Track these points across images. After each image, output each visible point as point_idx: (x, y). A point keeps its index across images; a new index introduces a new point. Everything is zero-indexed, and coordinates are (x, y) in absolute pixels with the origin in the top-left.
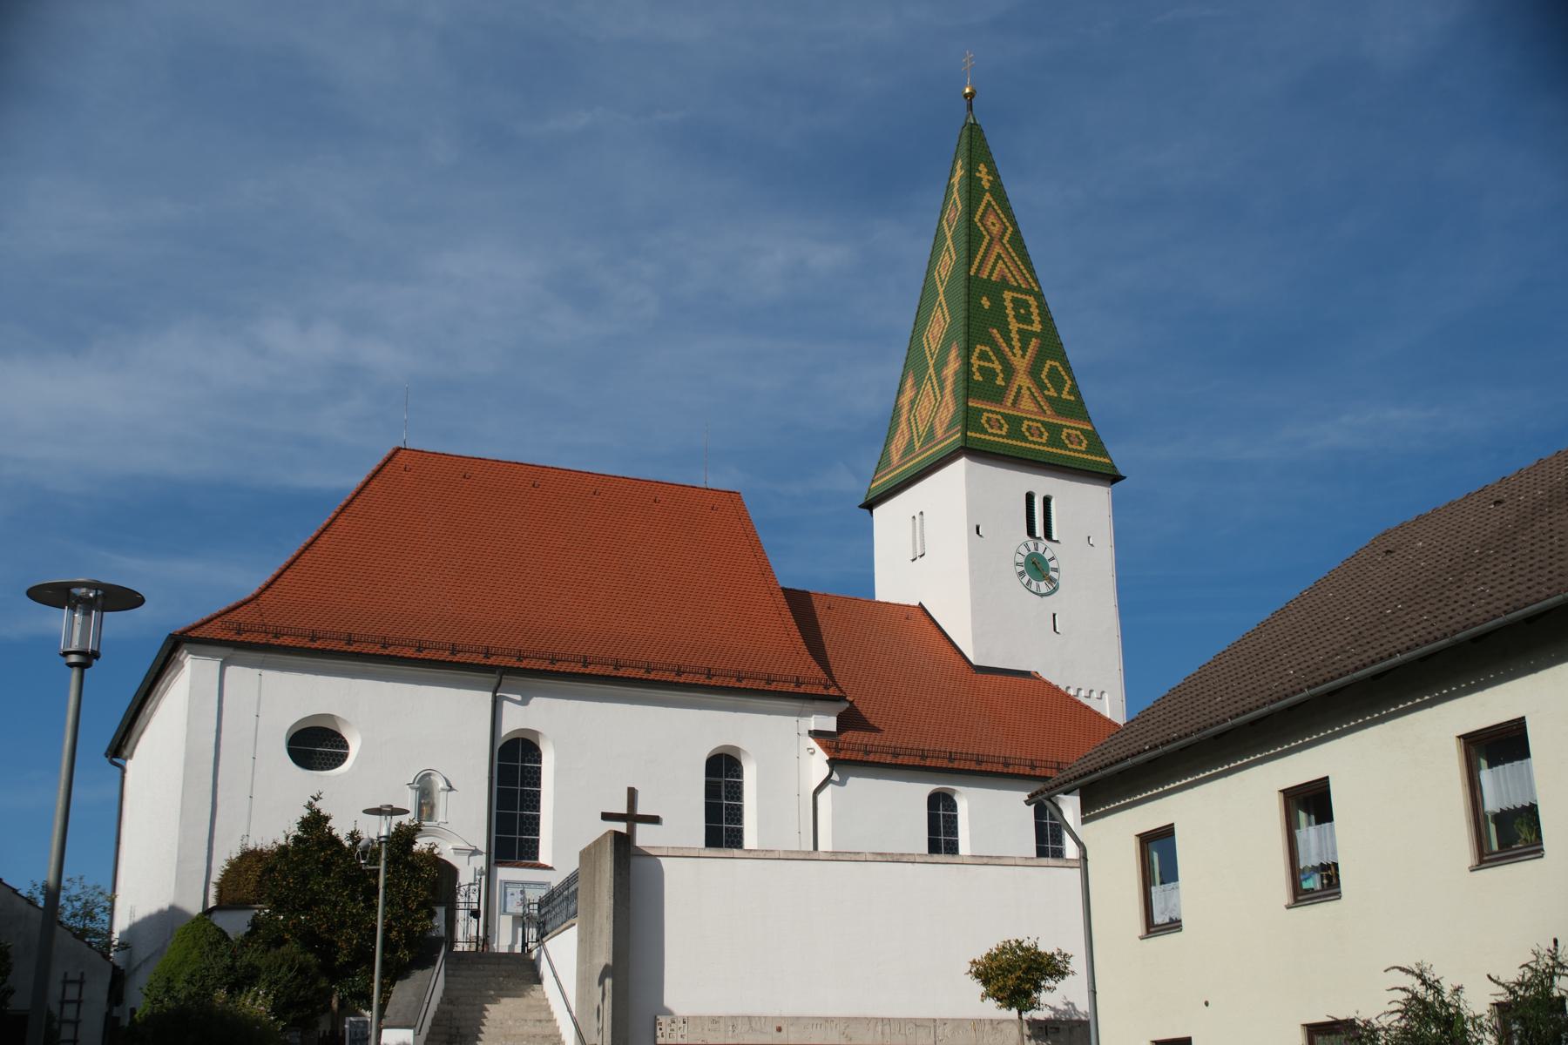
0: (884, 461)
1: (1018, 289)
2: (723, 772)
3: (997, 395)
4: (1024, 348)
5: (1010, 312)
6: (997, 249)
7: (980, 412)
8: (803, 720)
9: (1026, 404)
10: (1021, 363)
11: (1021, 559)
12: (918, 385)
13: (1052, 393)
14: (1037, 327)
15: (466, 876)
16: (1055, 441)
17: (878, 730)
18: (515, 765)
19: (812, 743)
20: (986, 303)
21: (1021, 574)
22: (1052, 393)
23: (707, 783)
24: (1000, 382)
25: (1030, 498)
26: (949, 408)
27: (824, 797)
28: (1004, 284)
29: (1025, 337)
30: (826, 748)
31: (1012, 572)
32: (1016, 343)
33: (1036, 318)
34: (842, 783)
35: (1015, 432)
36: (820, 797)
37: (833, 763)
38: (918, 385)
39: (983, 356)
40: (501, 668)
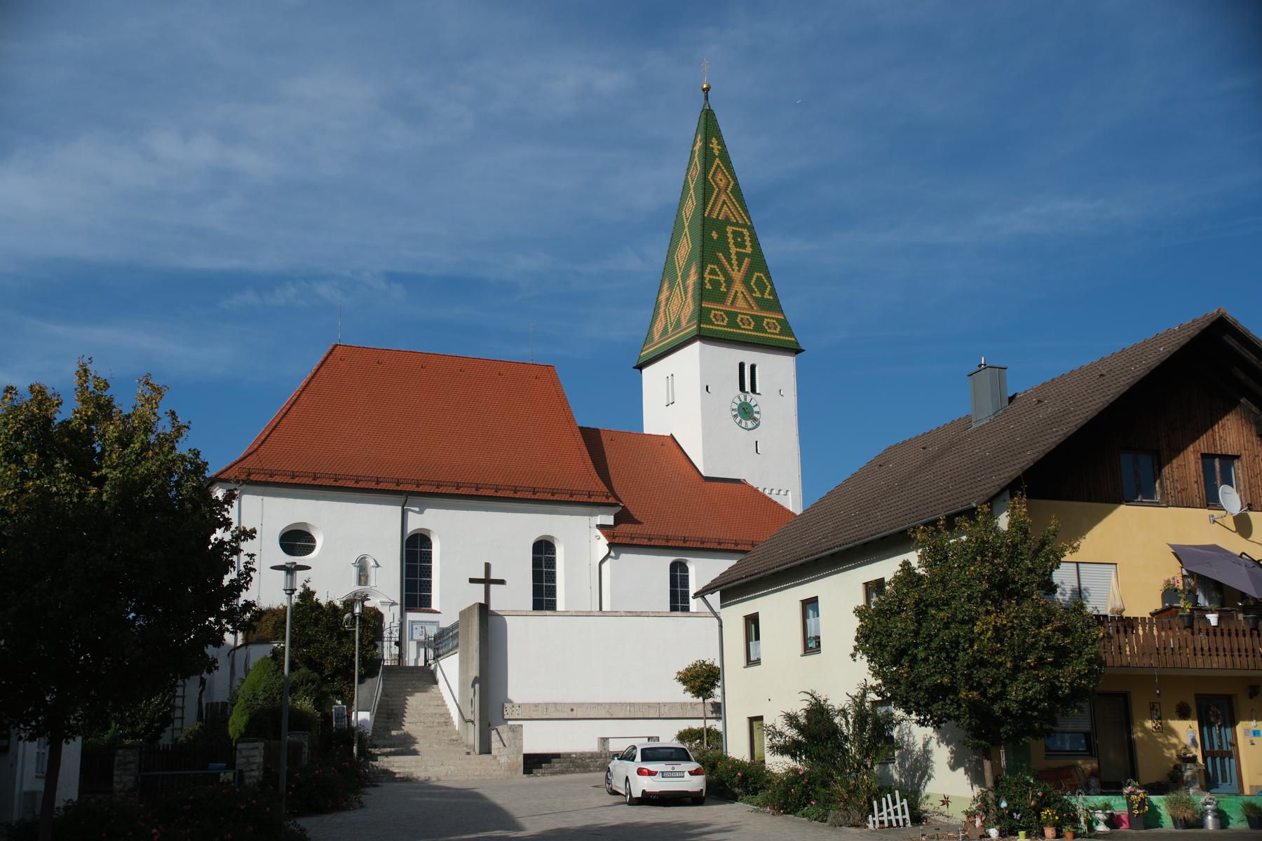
0: (648, 338)
1: (737, 224)
2: (543, 551)
3: (721, 298)
4: (740, 265)
5: (731, 241)
6: (723, 197)
7: (710, 310)
8: (593, 518)
9: (741, 303)
10: (737, 276)
11: (736, 407)
12: (671, 288)
13: (758, 295)
14: (749, 250)
15: (387, 620)
16: (758, 327)
17: (640, 523)
18: (416, 551)
19: (598, 532)
20: (715, 235)
21: (735, 416)
22: (758, 295)
23: (534, 559)
24: (723, 289)
25: (742, 366)
26: (689, 308)
27: (606, 566)
28: (727, 221)
29: (740, 257)
30: (607, 536)
31: (730, 415)
32: (734, 262)
33: (748, 244)
34: (617, 557)
35: (733, 323)
36: (603, 566)
37: (611, 545)
38: (671, 288)
39: (713, 272)
40: (408, 492)
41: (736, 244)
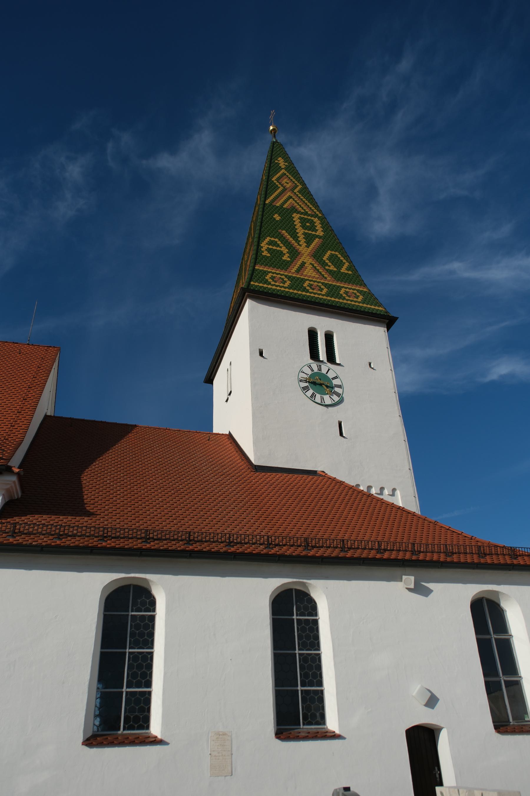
9: (309, 272)
13: (332, 268)
21: (305, 389)
22: (332, 268)
24: (286, 258)
25: (312, 334)
28: (294, 210)
31: (296, 387)
41: (304, 227)
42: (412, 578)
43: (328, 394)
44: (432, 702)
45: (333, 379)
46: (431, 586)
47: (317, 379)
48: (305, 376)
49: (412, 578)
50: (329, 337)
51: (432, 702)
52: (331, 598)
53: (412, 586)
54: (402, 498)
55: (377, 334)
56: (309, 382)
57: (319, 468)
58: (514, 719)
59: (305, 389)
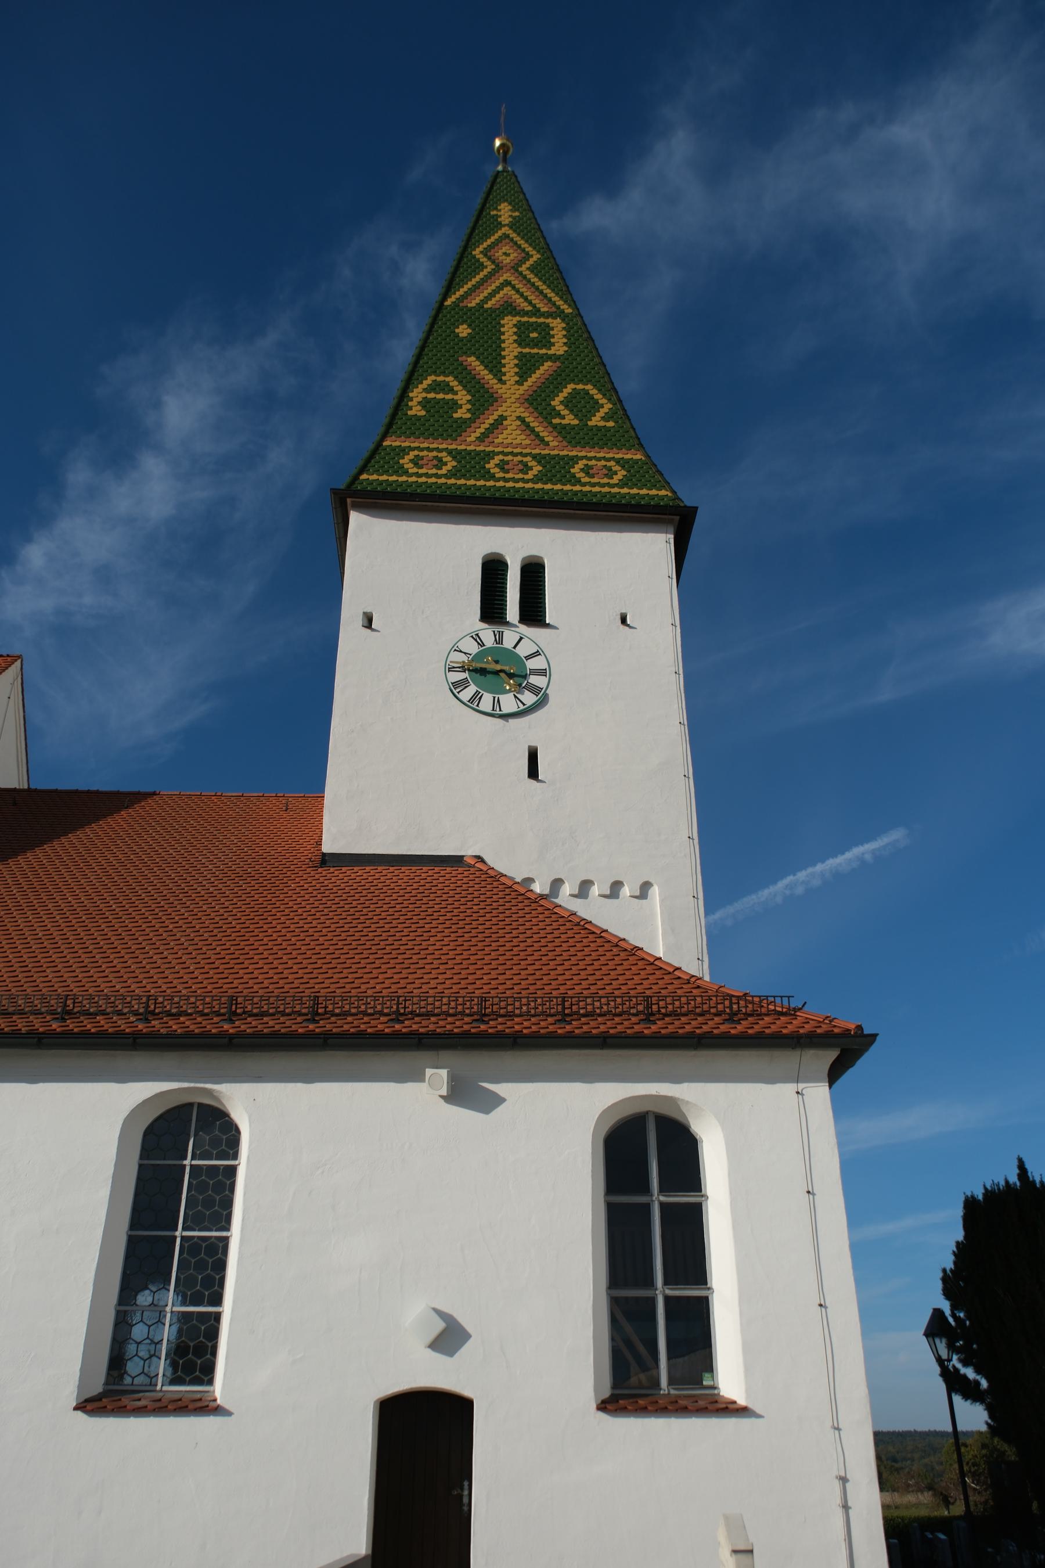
9: (511, 436)
21: (459, 686)
22: (570, 420)
31: (439, 682)
42: (444, 1073)
43: (510, 691)
44: (450, 1338)
45: (528, 658)
46: (500, 1089)
47: (488, 662)
48: (463, 658)
49: (444, 1073)
50: (533, 573)
51: (450, 1338)
52: (276, 1119)
53: (445, 1094)
54: (662, 901)
55: (651, 549)
56: (469, 670)
57: (468, 851)
58: (671, 1382)
59: (459, 686)
